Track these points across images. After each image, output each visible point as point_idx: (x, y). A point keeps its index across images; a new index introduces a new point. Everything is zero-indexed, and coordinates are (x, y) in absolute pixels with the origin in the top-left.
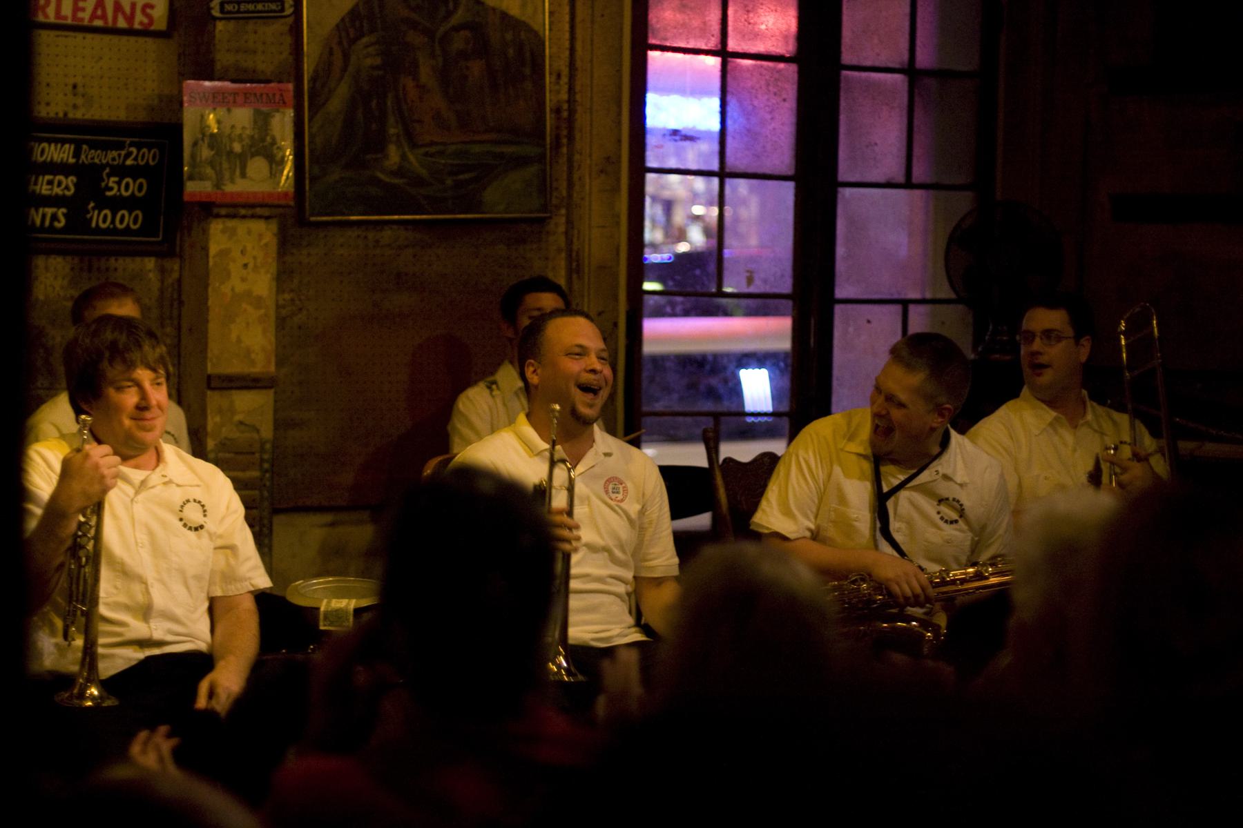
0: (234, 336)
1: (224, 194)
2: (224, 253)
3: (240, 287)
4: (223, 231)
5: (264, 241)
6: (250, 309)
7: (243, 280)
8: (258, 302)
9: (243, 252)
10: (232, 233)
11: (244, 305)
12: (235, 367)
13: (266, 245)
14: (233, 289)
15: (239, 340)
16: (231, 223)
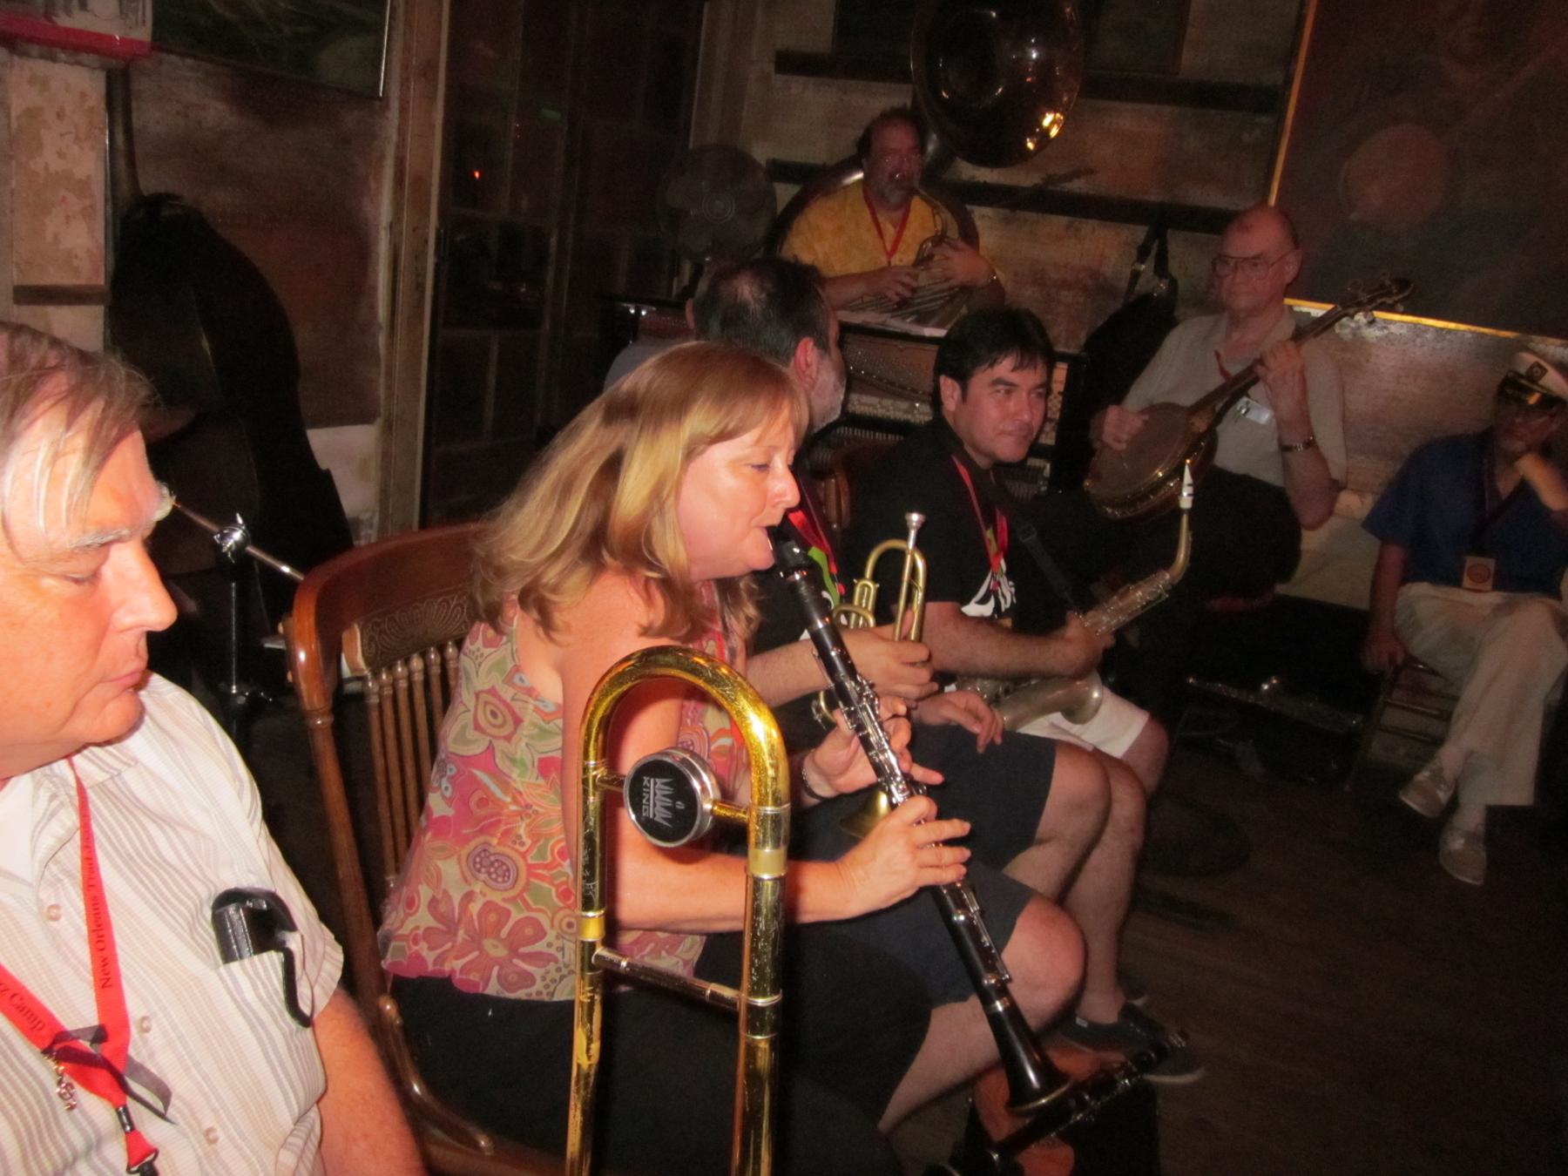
0: (49, 236)
1: (56, 28)
2: (32, 114)
3: (57, 165)
4: (32, 80)
5: (91, 103)
6: (71, 198)
7: (61, 155)
8: (82, 188)
9: (60, 115)
10: (43, 84)
11: (63, 192)
12: (54, 277)
13: (91, 109)
14: (46, 167)
15: (56, 237)
16: (42, 67)
